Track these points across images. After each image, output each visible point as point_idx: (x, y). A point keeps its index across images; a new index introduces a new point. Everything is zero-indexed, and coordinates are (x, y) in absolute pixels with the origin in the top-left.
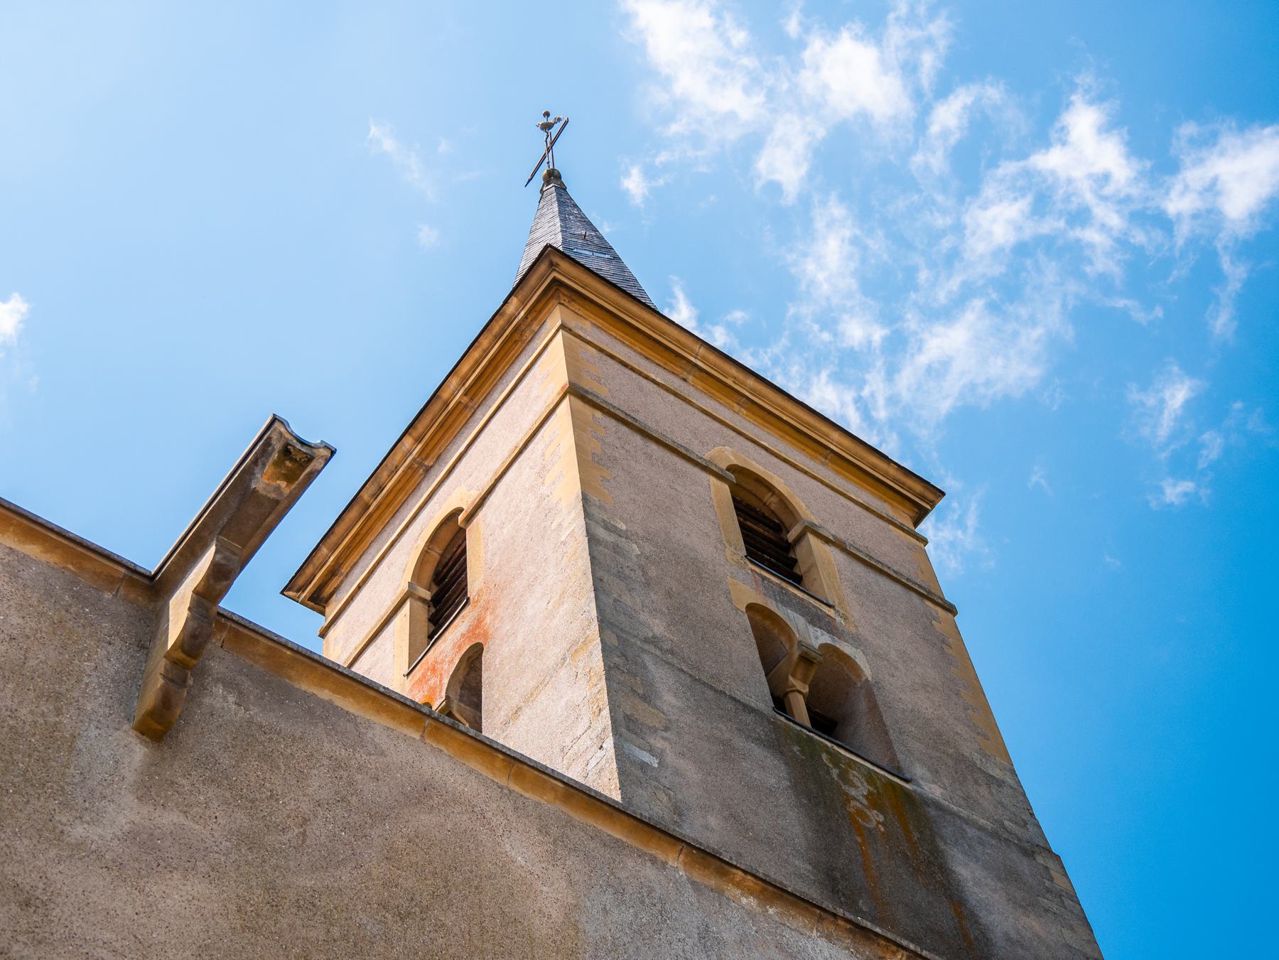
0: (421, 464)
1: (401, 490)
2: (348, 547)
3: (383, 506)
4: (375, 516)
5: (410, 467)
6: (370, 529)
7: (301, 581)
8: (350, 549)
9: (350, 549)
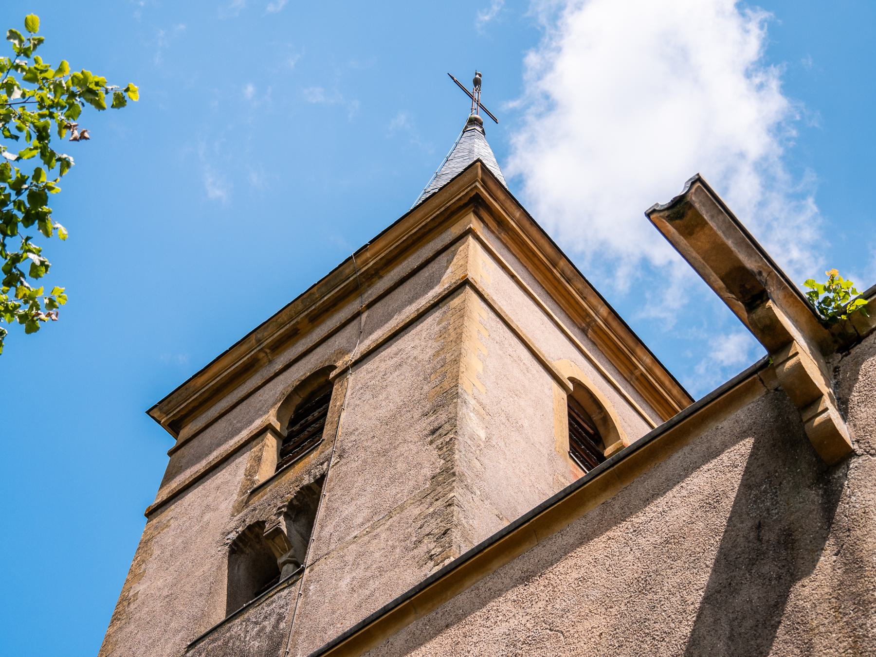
0: (588, 325)
1: (568, 302)
2: (524, 243)
3: (556, 284)
4: (549, 275)
5: (589, 315)
6: (537, 268)
7: (491, 184)
8: (521, 244)
9: (521, 244)
